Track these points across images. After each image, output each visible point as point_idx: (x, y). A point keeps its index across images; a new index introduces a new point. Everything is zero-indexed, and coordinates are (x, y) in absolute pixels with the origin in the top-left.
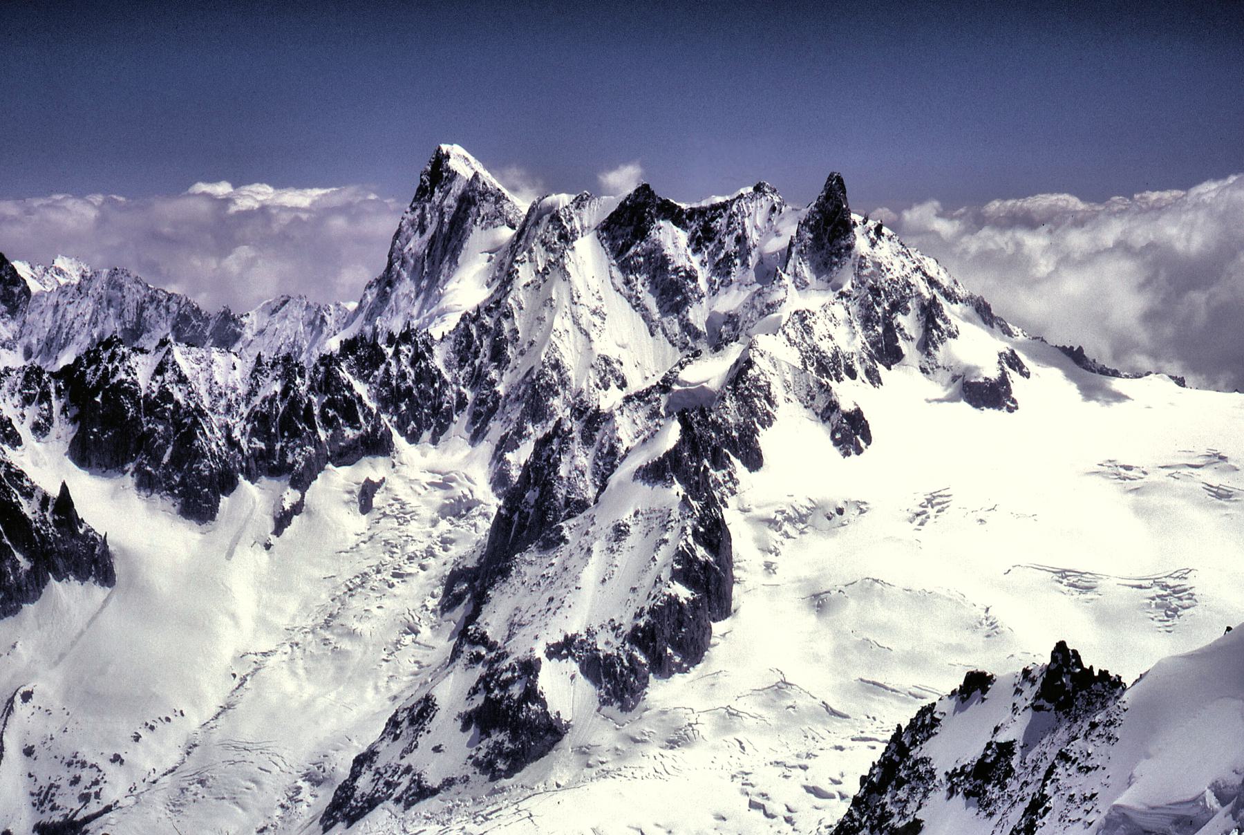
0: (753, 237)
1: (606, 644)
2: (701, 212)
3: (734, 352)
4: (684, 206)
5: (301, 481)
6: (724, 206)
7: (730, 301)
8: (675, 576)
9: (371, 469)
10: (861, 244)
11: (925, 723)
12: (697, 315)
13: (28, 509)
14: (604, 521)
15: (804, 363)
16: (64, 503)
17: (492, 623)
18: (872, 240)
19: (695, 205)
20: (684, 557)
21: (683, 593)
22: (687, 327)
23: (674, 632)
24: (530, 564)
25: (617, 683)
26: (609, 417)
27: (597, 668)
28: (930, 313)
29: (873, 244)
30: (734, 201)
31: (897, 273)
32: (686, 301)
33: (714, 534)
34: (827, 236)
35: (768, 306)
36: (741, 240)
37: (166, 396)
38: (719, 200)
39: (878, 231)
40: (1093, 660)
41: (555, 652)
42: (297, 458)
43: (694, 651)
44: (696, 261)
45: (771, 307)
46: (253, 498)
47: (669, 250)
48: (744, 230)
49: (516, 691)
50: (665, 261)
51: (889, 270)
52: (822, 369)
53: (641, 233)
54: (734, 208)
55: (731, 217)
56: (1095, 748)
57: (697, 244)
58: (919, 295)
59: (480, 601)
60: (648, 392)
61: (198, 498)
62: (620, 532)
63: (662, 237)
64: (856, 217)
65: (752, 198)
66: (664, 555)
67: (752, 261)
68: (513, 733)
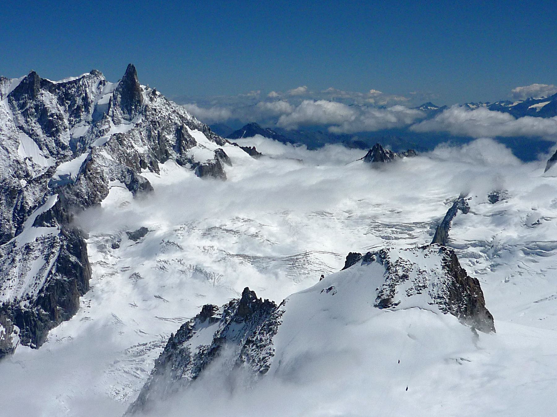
0: (91, 97)
2: (64, 85)
3: (84, 156)
4: (54, 82)
6: (75, 82)
7: (81, 130)
10: (146, 100)
12: (65, 138)
15: (120, 161)
18: (151, 98)
19: (60, 82)
22: (58, 143)
26: (21, 192)
28: (180, 133)
29: (151, 100)
30: (80, 79)
31: (165, 113)
32: (58, 131)
34: (129, 97)
35: (100, 132)
36: (85, 99)
38: (72, 79)
39: (154, 93)
44: (62, 108)
45: (102, 133)
47: (48, 105)
48: (86, 94)
50: (45, 110)
51: (160, 112)
52: (129, 162)
53: (33, 97)
54: (81, 82)
55: (79, 87)
57: (61, 101)
58: (176, 124)
60: (41, 177)
63: (44, 99)
64: (143, 87)
65: (89, 77)
67: (91, 110)
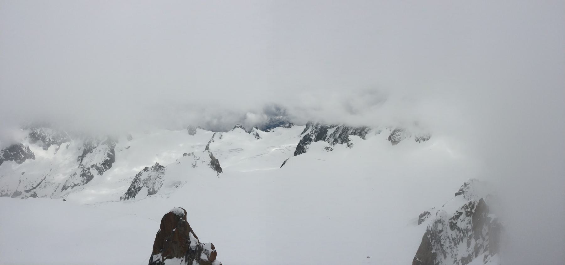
1: (99, 165)
5: (59, 145)
8: (108, 156)
9: (68, 143)
11: (140, 174)
13: (24, 149)
14: (98, 149)
16: (28, 148)
17: (84, 163)
20: (108, 154)
21: (108, 159)
23: (108, 164)
24: (89, 155)
25: (100, 172)
27: (97, 168)
33: (112, 151)
37: (41, 134)
40: (161, 165)
41: (92, 166)
42: (58, 142)
43: (110, 166)
46: (52, 147)
49: (87, 172)
56: (162, 176)
59: (82, 160)
61: (46, 147)
62: (100, 151)
66: (106, 154)
68: (87, 178)
